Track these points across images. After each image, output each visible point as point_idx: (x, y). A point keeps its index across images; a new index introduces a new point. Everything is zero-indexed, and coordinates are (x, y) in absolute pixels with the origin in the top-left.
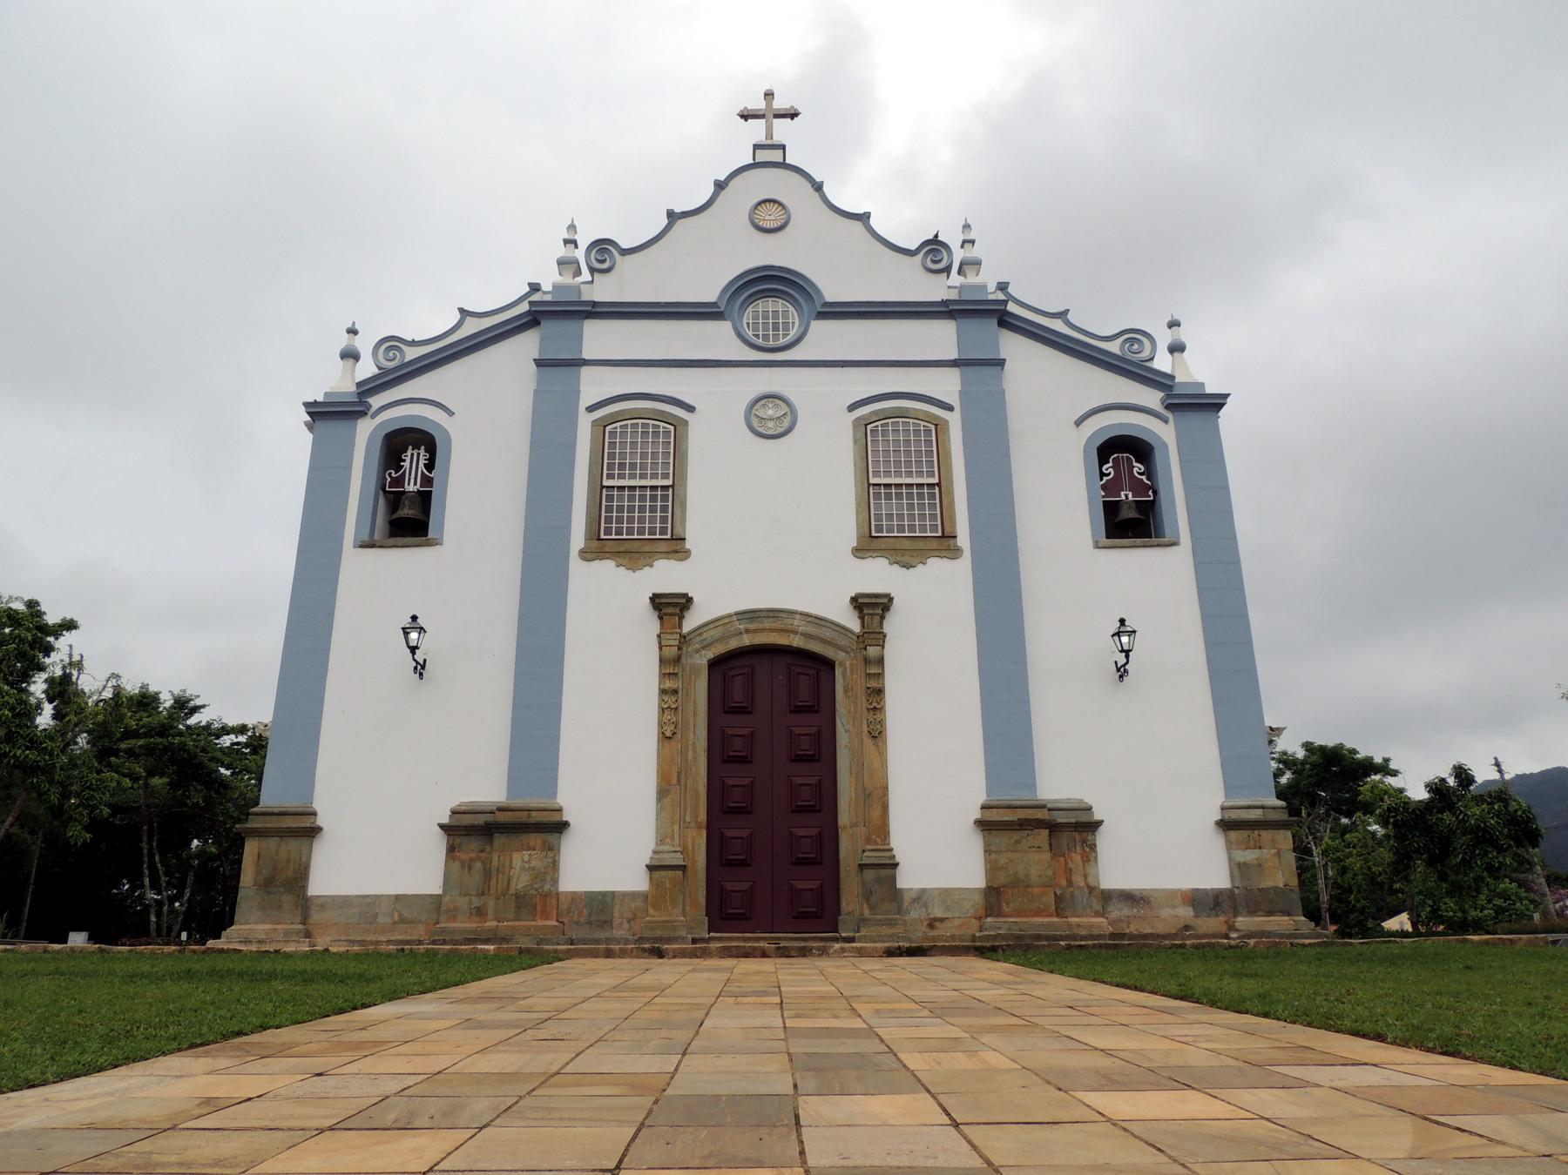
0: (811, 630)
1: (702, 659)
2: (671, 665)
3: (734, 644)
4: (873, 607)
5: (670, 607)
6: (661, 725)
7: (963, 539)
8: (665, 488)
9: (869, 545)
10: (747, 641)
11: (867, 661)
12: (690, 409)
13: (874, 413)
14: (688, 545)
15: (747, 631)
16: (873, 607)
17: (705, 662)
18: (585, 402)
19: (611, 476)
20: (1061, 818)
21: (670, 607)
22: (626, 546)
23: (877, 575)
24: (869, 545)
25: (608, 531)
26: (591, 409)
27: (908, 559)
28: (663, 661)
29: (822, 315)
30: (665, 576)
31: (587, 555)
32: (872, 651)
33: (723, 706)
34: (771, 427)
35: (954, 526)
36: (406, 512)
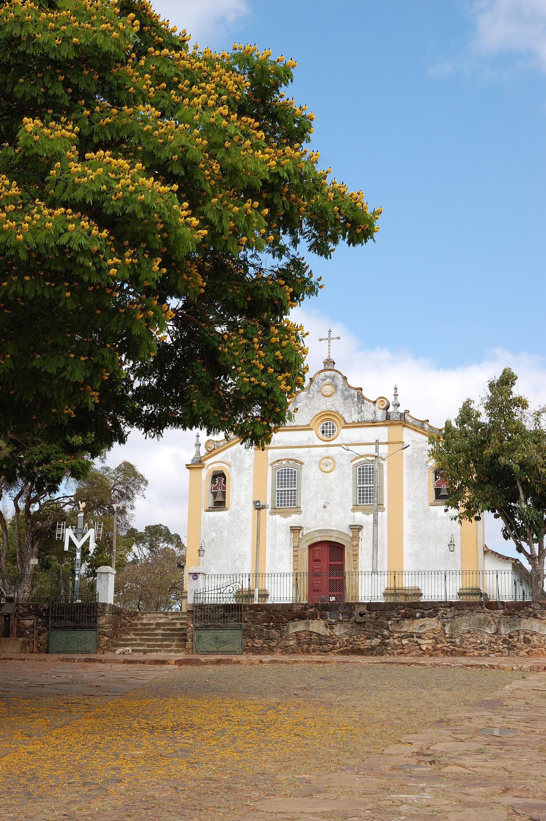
0: (337, 536)
1: (306, 546)
2: (296, 549)
3: (315, 541)
4: (357, 528)
5: (295, 530)
6: (294, 565)
7: (385, 506)
8: (295, 490)
9: (356, 508)
10: (319, 540)
11: (353, 546)
12: (302, 463)
13: (360, 462)
14: (302, 509)
15: (319, 536)
16: (357, 528)
17: (307, 546)
18: (270, 462)
19: (278, 487)
20: (407, 592)
21: (295, 530)
22: (284, 510)
23: (360, 517)
24: (356, 508)
25: (278, 505)
26: (271, 465)
27: (367, 512)
28: (294, 547)
29: (343, 428)
30: (294, 520)
31: (272, 514)
32: (354, 543)
33: (313, 560)
34: (327, 469)
35: (383, 501)
36: (220, 499)
